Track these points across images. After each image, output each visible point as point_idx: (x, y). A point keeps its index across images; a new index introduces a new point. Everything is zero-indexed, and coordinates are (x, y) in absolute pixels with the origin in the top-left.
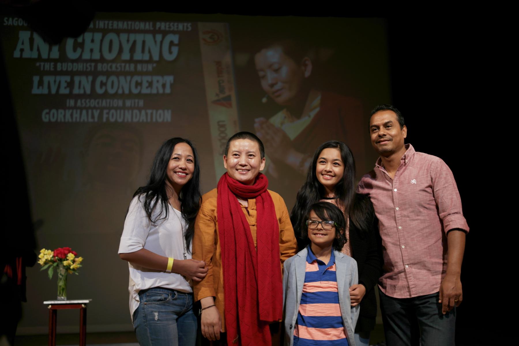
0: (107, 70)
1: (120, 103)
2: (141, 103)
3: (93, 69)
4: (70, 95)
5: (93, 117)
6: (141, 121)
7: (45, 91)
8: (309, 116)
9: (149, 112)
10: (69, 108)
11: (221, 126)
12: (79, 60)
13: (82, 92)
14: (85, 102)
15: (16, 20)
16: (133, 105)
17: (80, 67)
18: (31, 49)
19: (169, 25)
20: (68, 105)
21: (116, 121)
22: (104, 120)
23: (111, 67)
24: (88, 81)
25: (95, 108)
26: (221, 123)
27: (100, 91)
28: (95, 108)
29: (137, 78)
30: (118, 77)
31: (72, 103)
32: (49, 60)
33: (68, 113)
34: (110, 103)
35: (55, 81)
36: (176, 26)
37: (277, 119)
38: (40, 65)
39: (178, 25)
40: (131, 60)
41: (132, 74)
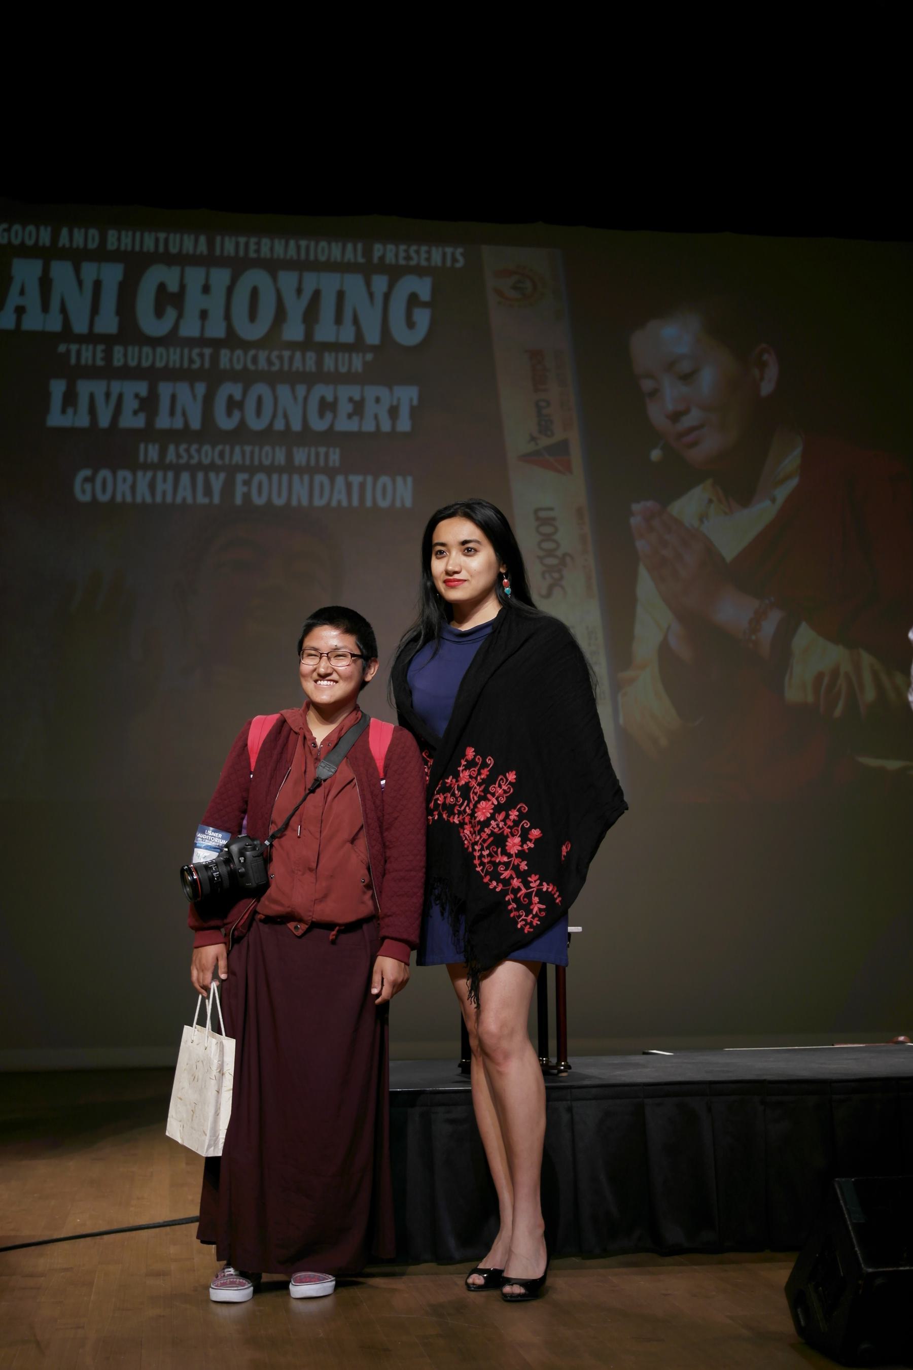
0: (245, 368)
1: (280, 456)
2: (335, 457)
3: (207, 365)
4: (148, 433)
5: (208, 491)
6: (334, 503)
7: (83, 421)
8: (773, 500)
9: (356, 479)
10: (146, 467)
12: (171, 339)
13: (179, 424)
14: (187, 450)
16: (313, 463)
17: (173, 357)
18: (45, 308)
19: (407, 251)
20: (142, 459)
22: (238, 500)
23: (255, 360)
24: (194, 396)
25: (212, 467)
26: (542, 514)
27: (226, 423)
28: (212, 467)
29: (323, 391)
30: (274, 391)
31: (152, 453)
32: (91, 338)
33: (143, 480)
34: (252, 453)
35: (108, 395)
36: (424, 256)
37: (689, 506)
38: (68, 351)
39: (429, 252)
40: (308, 343)
41: (310, 379)
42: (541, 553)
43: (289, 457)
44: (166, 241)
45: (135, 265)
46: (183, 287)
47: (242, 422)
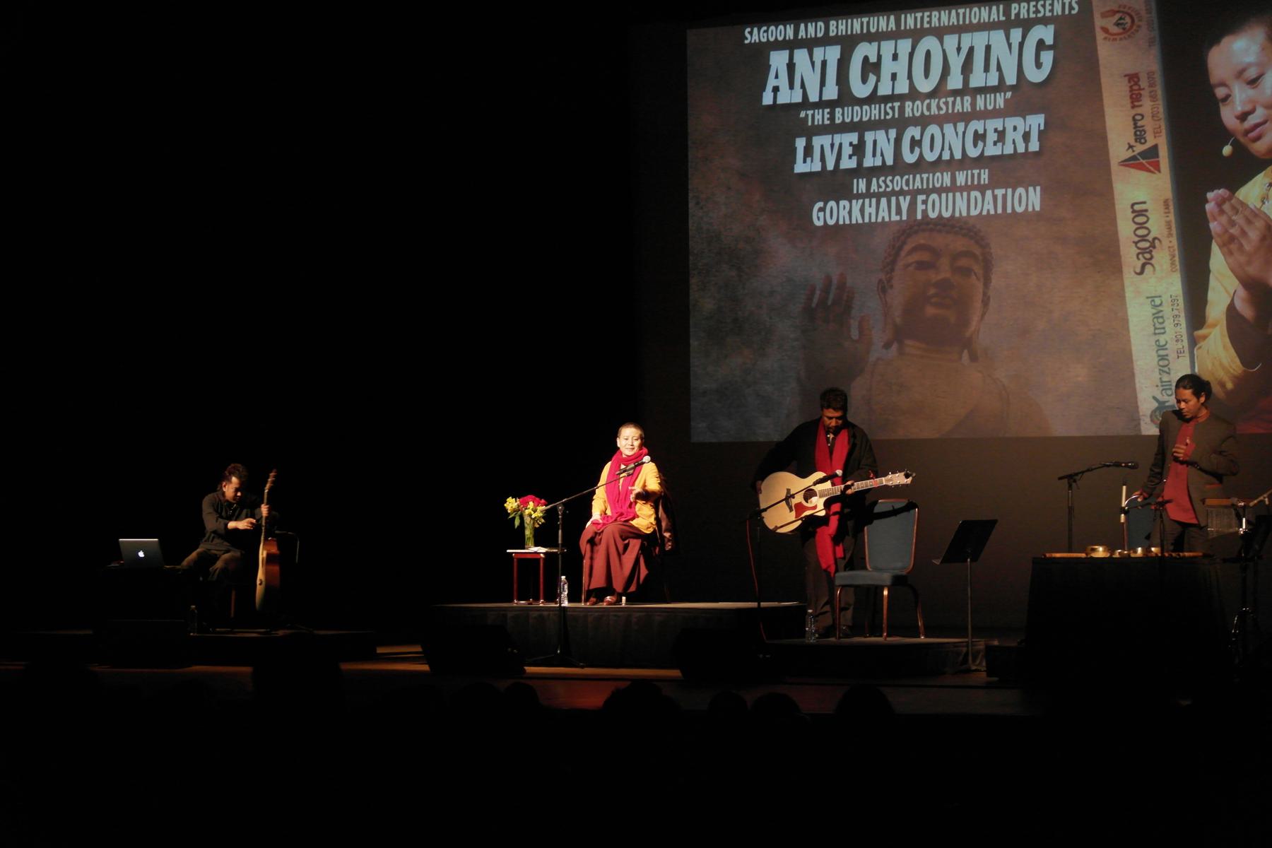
4: (859, 172)
5: (899, 212)
6: (985, 213)
7: (817, 167)
9: (1000, 192)
11: (1139, 212)
13: (879, 163)
14: (885, 182)
15: (766, 31)
17: (873, 112)
18: (791, 87)
19: (1036, 6)
21: (940, 216)
22: (919, 217)
25: (902, 193)
26: (1137, 207)
27: (910, 158)
28: (902, 193)
29: (977, 125)
31: (860, 185)
33: (856, 205)
35: (832, 145)
41: (966, 118)
42: (1137, 239)
43: (953, 179)
44: (868, 23)
45: (848, 44)
46: (879, 57)
47: (921, 154)
